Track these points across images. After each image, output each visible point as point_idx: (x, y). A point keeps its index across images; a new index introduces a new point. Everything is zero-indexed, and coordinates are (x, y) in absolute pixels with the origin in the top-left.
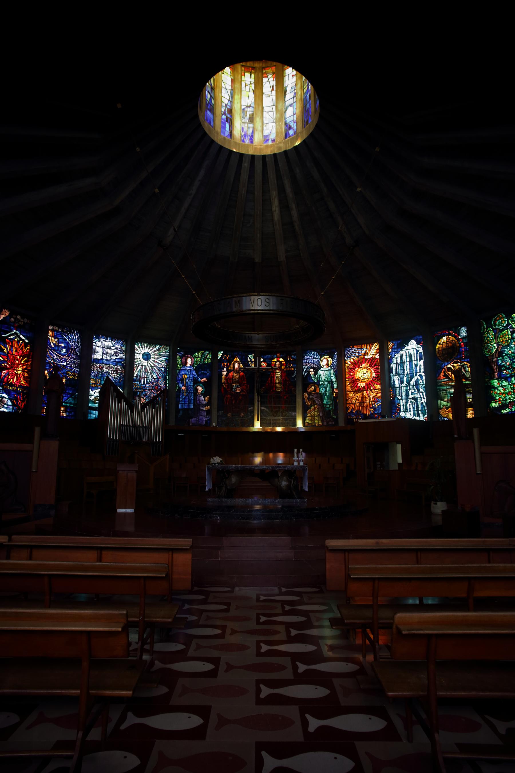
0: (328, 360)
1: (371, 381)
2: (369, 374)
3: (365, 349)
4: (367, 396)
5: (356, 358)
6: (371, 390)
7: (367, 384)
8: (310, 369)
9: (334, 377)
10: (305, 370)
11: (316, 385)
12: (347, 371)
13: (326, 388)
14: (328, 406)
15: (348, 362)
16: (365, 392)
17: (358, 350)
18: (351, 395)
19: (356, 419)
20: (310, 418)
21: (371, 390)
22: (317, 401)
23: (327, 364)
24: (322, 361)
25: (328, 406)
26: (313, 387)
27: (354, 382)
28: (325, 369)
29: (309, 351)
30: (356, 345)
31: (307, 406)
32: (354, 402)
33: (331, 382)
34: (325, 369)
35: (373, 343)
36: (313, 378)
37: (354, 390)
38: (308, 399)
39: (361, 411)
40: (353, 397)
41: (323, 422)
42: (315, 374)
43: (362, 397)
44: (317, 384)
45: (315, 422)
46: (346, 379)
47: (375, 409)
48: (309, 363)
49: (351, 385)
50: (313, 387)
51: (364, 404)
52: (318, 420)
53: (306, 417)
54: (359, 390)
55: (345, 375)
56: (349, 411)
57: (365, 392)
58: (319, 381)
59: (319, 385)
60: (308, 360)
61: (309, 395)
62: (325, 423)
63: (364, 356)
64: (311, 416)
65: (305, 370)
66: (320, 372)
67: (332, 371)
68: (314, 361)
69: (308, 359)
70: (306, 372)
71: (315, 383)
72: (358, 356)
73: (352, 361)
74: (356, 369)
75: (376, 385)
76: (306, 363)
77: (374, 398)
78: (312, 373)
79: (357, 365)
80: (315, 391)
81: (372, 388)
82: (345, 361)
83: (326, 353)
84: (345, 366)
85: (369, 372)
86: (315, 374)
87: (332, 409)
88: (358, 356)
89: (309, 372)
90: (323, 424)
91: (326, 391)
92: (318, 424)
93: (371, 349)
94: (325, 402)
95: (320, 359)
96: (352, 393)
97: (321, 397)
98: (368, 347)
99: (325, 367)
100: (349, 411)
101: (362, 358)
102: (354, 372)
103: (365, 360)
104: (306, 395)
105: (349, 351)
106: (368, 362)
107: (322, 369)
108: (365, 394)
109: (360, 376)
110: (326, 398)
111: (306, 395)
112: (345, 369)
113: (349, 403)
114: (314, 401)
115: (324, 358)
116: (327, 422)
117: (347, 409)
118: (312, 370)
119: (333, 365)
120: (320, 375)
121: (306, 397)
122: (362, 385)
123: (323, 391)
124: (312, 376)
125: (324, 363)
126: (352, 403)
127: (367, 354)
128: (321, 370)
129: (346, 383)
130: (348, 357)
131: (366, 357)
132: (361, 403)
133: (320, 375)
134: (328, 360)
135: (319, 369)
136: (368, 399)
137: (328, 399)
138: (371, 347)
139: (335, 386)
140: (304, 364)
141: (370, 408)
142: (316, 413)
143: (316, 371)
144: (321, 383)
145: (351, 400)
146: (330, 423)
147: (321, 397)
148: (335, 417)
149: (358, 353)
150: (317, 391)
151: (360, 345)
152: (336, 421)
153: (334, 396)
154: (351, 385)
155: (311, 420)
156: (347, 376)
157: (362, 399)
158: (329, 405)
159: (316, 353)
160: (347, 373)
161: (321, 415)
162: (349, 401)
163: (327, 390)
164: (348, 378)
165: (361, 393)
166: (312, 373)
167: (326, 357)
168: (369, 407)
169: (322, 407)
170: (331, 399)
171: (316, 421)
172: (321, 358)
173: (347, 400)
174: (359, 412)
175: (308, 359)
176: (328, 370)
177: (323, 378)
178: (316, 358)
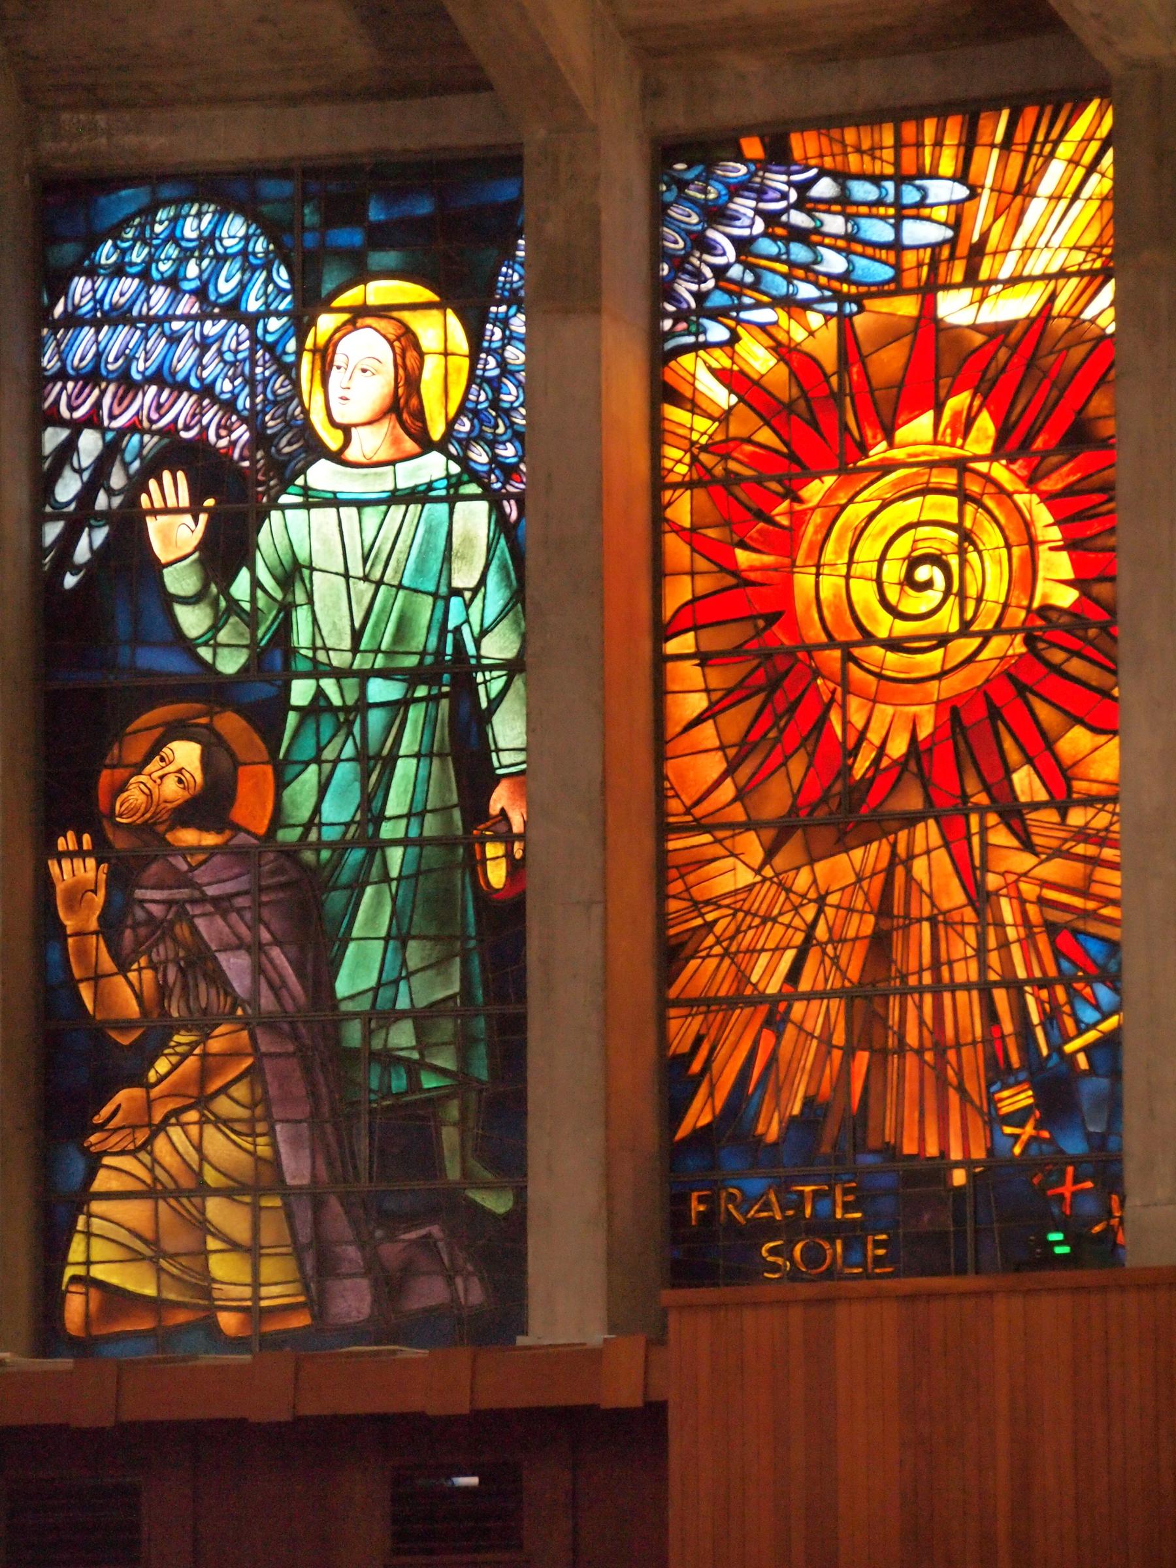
0: (407, 345)
1: (1014, 680)
2: (991, 575)
3: (943, 191)
4: (954, 896)
5: (814, 332)
6: (1013, 814)
7: (952, 713)
8: (152, 468)
9: (496, 596)
10: (68, 488)
11: (231, 724)
12: (682, 510)
13: (376, 765)
14: (402, 1037)
15: (699, 373)
16: (928, 833)
17: (842, 202)
18: (733, 875)
19: (793, 1229)
20: (135, 1213)
21: (1013, 814)
22: (236, 967)
23: (403, 408)
24: (325, 356)
25: (402, 1037)
26: (186, 754)
27: (784, 677)
28: (371, 480)
29: (130, 198)
30: (828, 123)
31: (100, 1033)
32: (768, 974)
33: (449, 674)
34: (371, 480)
35: (1064, 101)
36: (193, 621)
37: (776, 799)
38: (110, 926)
39: (859, 1123)
40: (773, 910)
41: (318, 1266)
42: (226, 550)
43: (884, 910)
44: (256, 703)
45: (204, 1285)
46: (663, 631)
47: (1056, 1092)
48: (129, 386)
49: (737, 720)
50: (186, 754)
51: (911, 1020)
52: (253, 1251)
53: (82, 1198)
54: (846, 808)
55: (659, 573)
56: (700, 1114)
57: (928, 833)
58: (275, 655)
59: (268, 716)
60: (119, 339)
61: (123, 877)
62: (353, 1300)
63: (928, 292)
64: (151, 1193)
65: (68, 488)
66: (287, 530)
67: (474, 518)
68: (215, 356)
69: (119, 316)
70: (81, 516)
71: (214, 690)
72: (847, 294)
73: (758, 358)
74: (815, 491)
75: (1076, 741)
76: (92, 377)
77: (1061, 933)
78: (175, 536)
79: (822, 421)
80: (209, 804)
81: (1026, 782)
82: (661, 356)
83: (378, 237)
84: (657, 433)
85: (991, 537)
86: (226, 550)
87: (462, 1079)
88: (847, 294)
89: (129, 525)
90: (317, 1303)
91: (371, 810)
92: (254, 1313)
93: (1024, 190)
94: (356, 975)
95: (301, 324)
96: (752, 845)
97: (305, 897)
98: (988, 164)
99: (371, 442)
100: (700, 1114)
101: (891, 333)
102: (785, 542)
103: (937, 363)
104: (77, 871)
105: (717, 215)
106: (989, 393)
107: (322, 476)
108: (934, 871)
109: (864, 593)
110: (373, 913)
111: (77, 871)
112: (658, 480)
113: (705, 1003)
114: (199, 963)
115: (360, 313)
116: (390, 1285)
117: (677, 1079)
118: (173, 488)
119: (481, 416)
120: (294, 573)
121: (77, 895)
122: (889, 729)
123: (339, 809)
124: (180, 580)
125: (354, 380)
126: (743, 997)
127: (965, 258)
128: (311, 500)
129: (660, 692)
130: (703, 310)
131: (955, 307)
132: (868, 1002)
133: (294, 573)
134: (407, 345)
135: (285, 472)
136: (962, 946)
137: (398, 937)
138: (1036, 156)
139: (509, 731)
140: (60, 395)
141: (999, 1073)
142: (216, 1143)
143: (238, 493)
144: (301, 692)
145: (738, 957)
146: (429, 1292)
147: (305, 897)
148: (497, 1203)
149: (850, 243)
150: (251, 809)
151: (873, 117)
152: (502, 1250)
153: (483, 895)
154: (737, 720)
155: (149, 1249)
156: (679, 592)
157: (880, 943)
158: (423, 1018)
159: (235, 228)
160: (677, 549)
161: (297, 1169)
162: (703, 973)
163: (397, 803)
164: (693, 616)
165: (867, 857)
166: (175, 536)
167: (380, 292)
168: (972, 1062)
169: (314, 1047)
170: (447, 943)
171: (225, 1268)
172: (308, 303)
173: (672, 954)
174: (833, 1134)
175: (119, 316)
176: (418, 496)
177: (328, 617)
178: (232, 310)
